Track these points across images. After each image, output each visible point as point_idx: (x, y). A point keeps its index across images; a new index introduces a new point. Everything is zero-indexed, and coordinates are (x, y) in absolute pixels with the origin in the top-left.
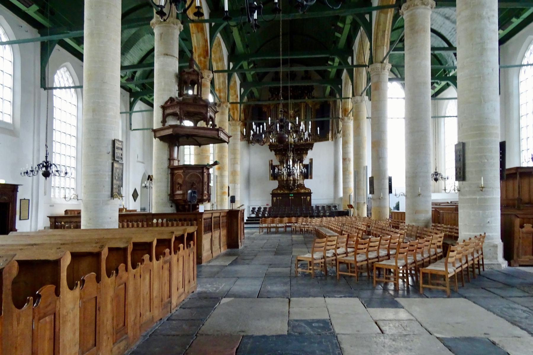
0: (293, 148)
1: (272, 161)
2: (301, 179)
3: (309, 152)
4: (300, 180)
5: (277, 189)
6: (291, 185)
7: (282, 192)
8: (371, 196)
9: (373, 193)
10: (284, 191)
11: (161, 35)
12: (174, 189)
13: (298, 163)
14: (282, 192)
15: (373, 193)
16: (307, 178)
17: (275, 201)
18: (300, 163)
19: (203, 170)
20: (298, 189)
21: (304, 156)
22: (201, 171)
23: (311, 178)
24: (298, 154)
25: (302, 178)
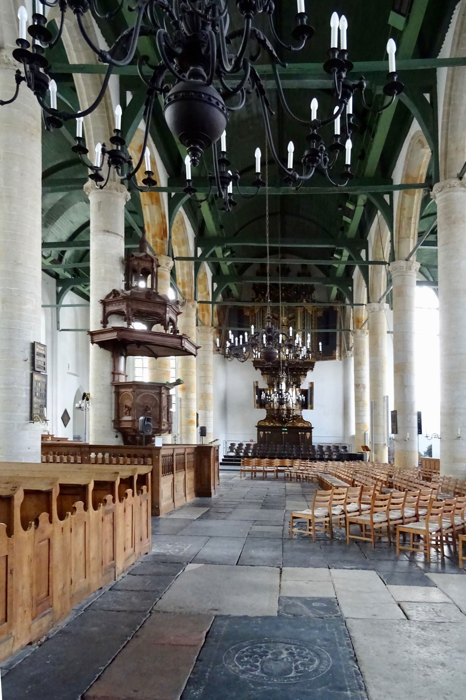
0: (287, 367)
4: (296, 410)
5: (264, 420)
6: (284, 416)
7: (272, 424)
8: (393, 436)
9: (397, 433)
11: (99, 204)
12: (120, 414)
13: (294, 387)
14: (272, 424)
17: (262, 436)
18: (297, 387)
20: (293, 422)
21: (302, 378)
23: (312, 408)
24: (294, 376)
25: (299, 408)
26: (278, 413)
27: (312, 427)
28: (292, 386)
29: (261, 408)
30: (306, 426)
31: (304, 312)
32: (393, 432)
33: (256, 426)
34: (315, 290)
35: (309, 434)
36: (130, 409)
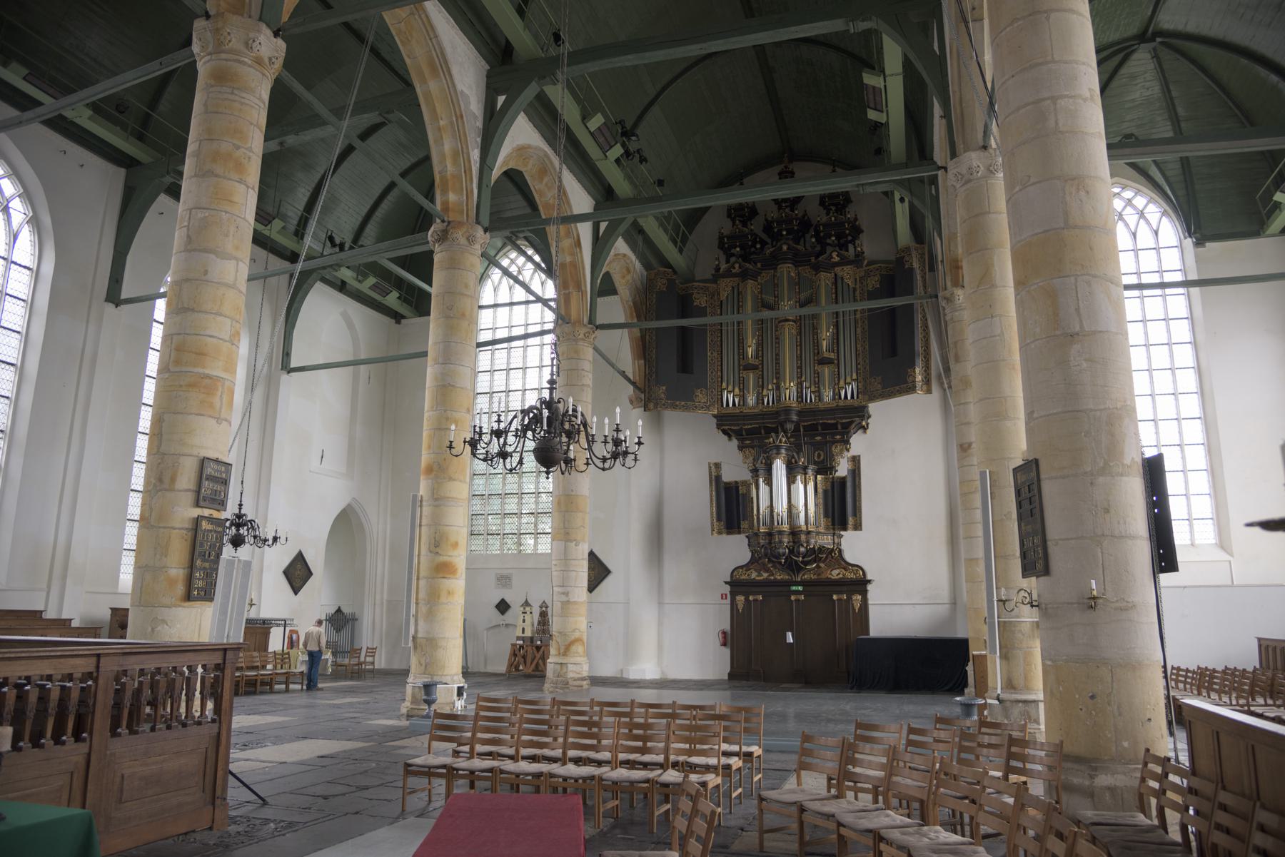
1: (718, 466)
2: (821, 529)
4: (818, 533)
5: (747, 567)
7: (765, 575)
8: (1032, 583)
9: (1046, 571)
13: (810, 472)
14: (765, 575)
15: (1046, 571)
17: (740, 606)
18: (818, 472)
20: (818, 567)
23: (858, 527)
24: (818, 445)
25: (827, 528)
26: (770, 543)
27: (869, 577)
28: (805, 469)
29: (729, 533)
30: (852, 576)
31: (835, 283)
32: (1027, 571)
33: (726, 583)
34: (862, 231)
35: (859, 597)
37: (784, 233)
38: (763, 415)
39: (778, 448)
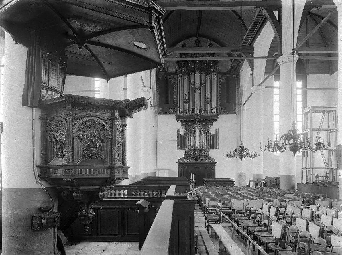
0: (199, 120)
3: (214, 123)
5: (183, 158)
7: (188, 161)
10: (190, 160)
16: (213, 148)
19: (113, 114)
22: (108, 115)
24: (204, 126)
33: (177, 163)
36: (63, 146)
37: (206, 64)
38: (189, 116)
39: (198, 126)
